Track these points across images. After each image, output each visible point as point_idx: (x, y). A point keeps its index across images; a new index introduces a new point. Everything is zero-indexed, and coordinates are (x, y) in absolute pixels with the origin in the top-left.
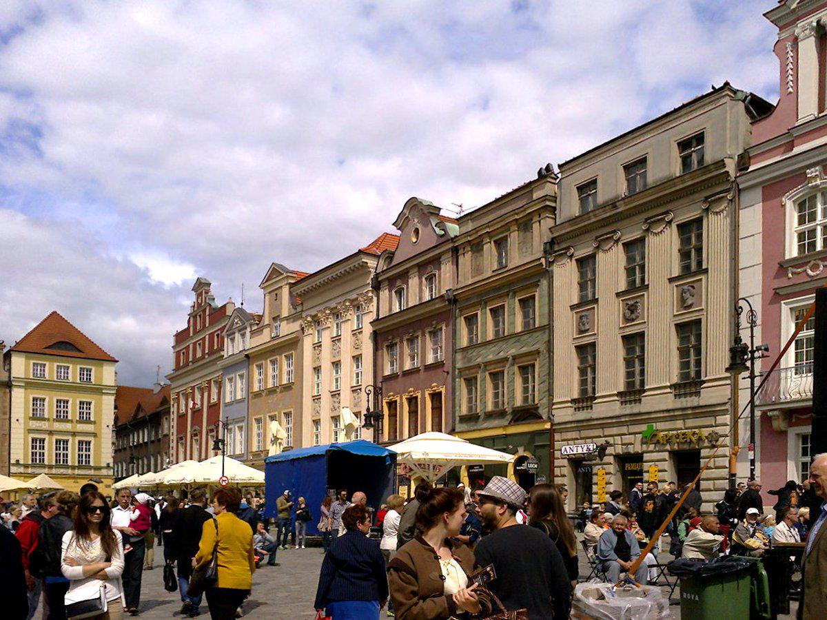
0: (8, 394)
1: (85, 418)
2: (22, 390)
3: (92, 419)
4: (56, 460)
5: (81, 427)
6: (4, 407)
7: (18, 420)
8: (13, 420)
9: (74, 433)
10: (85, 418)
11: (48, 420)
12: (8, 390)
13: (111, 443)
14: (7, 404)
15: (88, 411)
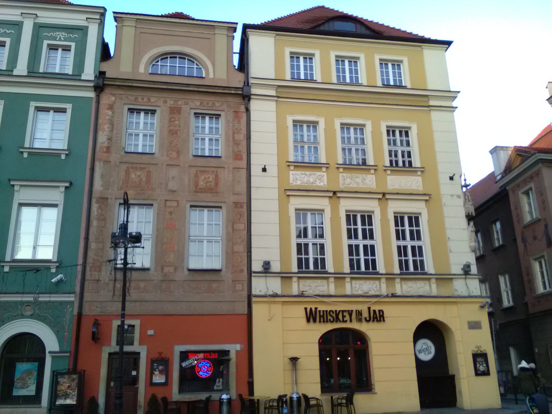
0: (244, 115)
1: (400, 164)
2: (271, 106)
3: (417, 163)
4: (351, 261)
5: (396, 182)
6: (237, 143)
7: (264, 170)
8: (256, 170)
9: (384, 194)
10: (400, 164)
11: (327, 166)
12: (243, 108)
13: (463, 214)
14: (242, 137)
15: (406, 149)
